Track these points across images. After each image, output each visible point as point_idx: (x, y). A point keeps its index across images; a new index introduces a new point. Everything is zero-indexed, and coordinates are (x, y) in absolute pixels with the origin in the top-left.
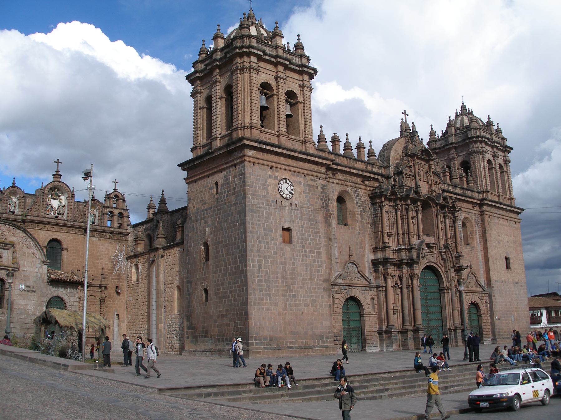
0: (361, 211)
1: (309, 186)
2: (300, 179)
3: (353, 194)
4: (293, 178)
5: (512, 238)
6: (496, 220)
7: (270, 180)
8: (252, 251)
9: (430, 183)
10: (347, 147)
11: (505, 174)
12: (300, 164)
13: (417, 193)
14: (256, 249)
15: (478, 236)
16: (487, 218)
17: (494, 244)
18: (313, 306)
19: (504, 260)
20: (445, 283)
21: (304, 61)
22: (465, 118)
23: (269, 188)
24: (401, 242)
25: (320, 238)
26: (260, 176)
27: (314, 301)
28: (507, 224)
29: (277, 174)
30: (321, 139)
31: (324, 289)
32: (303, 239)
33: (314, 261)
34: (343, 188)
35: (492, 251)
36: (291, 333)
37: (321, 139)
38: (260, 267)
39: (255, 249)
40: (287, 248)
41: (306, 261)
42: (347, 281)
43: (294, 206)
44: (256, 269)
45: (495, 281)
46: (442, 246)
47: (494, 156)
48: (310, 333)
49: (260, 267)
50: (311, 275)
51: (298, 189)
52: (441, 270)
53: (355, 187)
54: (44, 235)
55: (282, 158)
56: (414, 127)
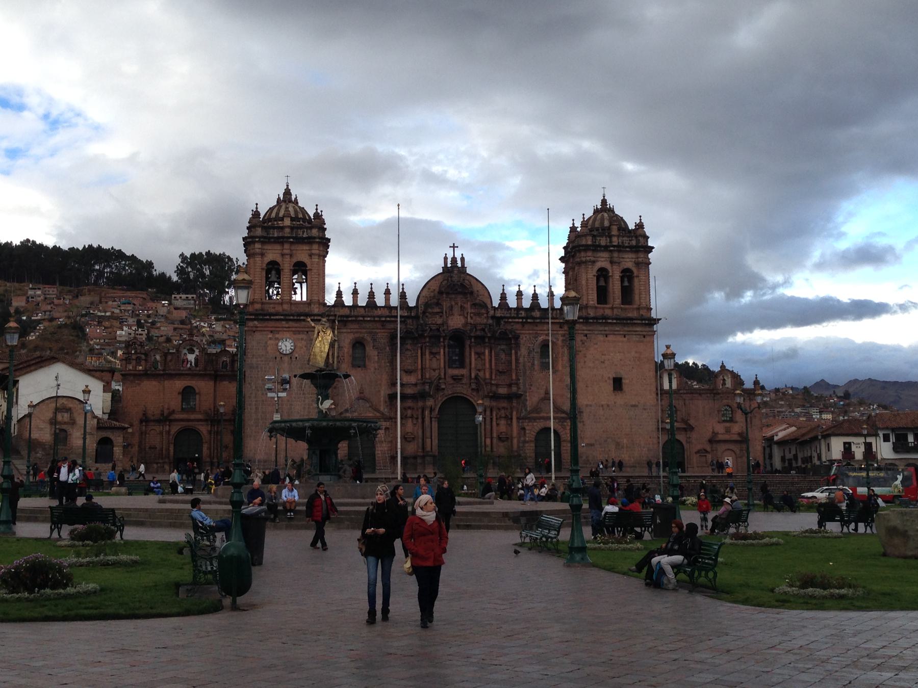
3: (369, 339)
4: (296, 336)
6: (601, 338)
7: (270, 342)
8: (250, 397)
10: (371, 295)
11: (636, 280)
13: (438, 330)
14: (253, 395)
15: (566, 358)
16: (579, 338)
17: (591, 365)
19: (612, 382)
21: (315, 232)
22: (606, 215)
23: (269, 348)
24: (420, 377)
28: (625, 339)
29: (277, 336)
30: (339, 294)
34: (357, 335)
35: (582, 374)
37: (339, 294)
39: (253, 395)
42: (356, 414)
43: (294, 359)
45: (587, 405)
46: (473, 376)
47: (612, 262)
51: (299, 345)
54: (179, 384)
56: (463, 259)
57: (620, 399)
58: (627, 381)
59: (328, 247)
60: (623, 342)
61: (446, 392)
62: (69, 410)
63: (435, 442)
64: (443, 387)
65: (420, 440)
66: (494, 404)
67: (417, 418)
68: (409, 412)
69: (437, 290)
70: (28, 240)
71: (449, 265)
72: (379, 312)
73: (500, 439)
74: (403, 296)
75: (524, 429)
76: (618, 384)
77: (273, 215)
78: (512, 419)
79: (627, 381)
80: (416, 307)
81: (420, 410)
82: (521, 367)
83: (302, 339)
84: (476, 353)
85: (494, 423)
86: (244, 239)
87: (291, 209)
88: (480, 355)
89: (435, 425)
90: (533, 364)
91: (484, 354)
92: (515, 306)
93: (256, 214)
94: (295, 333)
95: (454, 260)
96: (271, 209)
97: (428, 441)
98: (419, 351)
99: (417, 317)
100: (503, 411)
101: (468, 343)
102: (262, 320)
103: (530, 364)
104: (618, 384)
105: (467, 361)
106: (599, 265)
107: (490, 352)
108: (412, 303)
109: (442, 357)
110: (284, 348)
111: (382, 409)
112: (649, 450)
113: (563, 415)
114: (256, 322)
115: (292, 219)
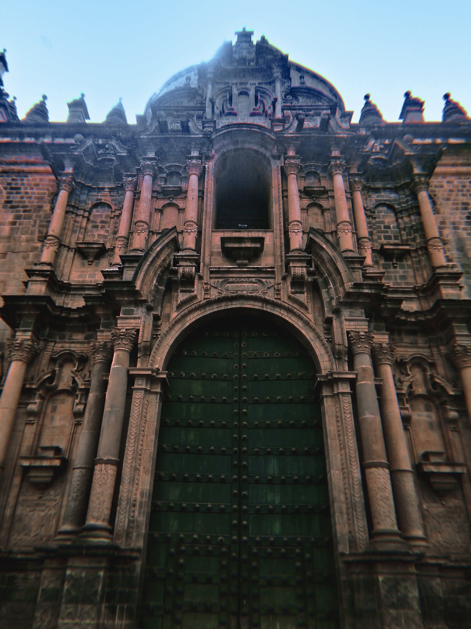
0: (18, 217)
9: (270, 111)
20: (325, 363)
52: (306, 322)
53: (13, 172)
61: (197, 289)
63: (140, 483)
65: (76, 476)
66: (382, 339)
67: (86, 392)
68: (67, 374)
73: (423, 478)
81: (99, 357)
84: (306, 192)
85: (394, 409)
88: (315, 197)
89: (147, 410)
91: (326, 193)
97: (104, 476)
98: (128, 195)
100: (416, 375)
101: (276, 165)
105: (276, 210)
107: (350, 191)
109: (193, 194)
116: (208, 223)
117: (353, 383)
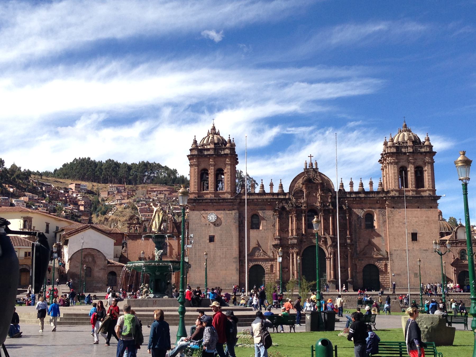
1: (226, 214)
2: (220, 212)
5: (424, 218)
12: (222, 204)
17: (397, 225)
18: (226, 270)
25: (232, 237)
26: (197, 214)
27: (227, 268)
31: (234, 262)
32: (221, 239)
33: (227, 249)
36: (212, 282)
38: (195, 254)
40: (212, 244)
41: (223, 249)
44: (193, 256)
45: (395, 250)
48: (224, 282)
49: (195, 254)
50: (226, 256)
55: (211, 204)
57: (416, 246)
58: (421, 235)
59: (237, 159)
60: (417, 211)
62: (93, 256)
64: (304, 240)
69: (301, 182)
70: (110, 160)
71: (308, 167)
72: (267, 197)
74: (281, 186)
75: (356, 265)
76: (414, 237)
77: (205, 142)
78: (347, 259)
79: (421, 235)
80: (289, 193)
82: (353, 227)
83: (221, 213)
86: (188, 156)
87: (215, 138)
90: (361, 225)
92: (349, 191)
93: (195, 142)
94: (217, 210)
95: (312, 164)
96: (204, 139)
99: (289, 199)
102: (198, 202)
103: (359, 225)
104: (414, 237)
106: (401, 164)
108: (286, 190)
110: (211, 219)
111: (269, 254)
112: (436, 278)
113: (380, 256)
114: (194, 204)
115: (215, 144)
116: (307, 227)
117: (330, 259)
